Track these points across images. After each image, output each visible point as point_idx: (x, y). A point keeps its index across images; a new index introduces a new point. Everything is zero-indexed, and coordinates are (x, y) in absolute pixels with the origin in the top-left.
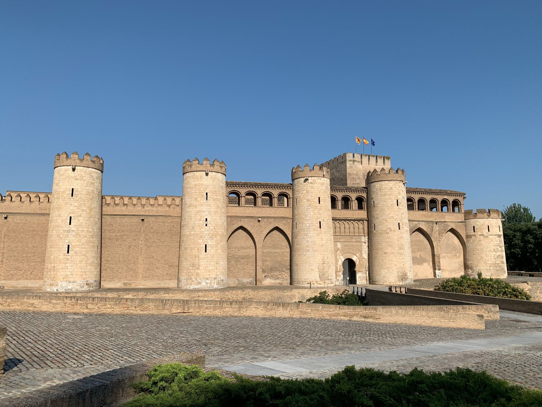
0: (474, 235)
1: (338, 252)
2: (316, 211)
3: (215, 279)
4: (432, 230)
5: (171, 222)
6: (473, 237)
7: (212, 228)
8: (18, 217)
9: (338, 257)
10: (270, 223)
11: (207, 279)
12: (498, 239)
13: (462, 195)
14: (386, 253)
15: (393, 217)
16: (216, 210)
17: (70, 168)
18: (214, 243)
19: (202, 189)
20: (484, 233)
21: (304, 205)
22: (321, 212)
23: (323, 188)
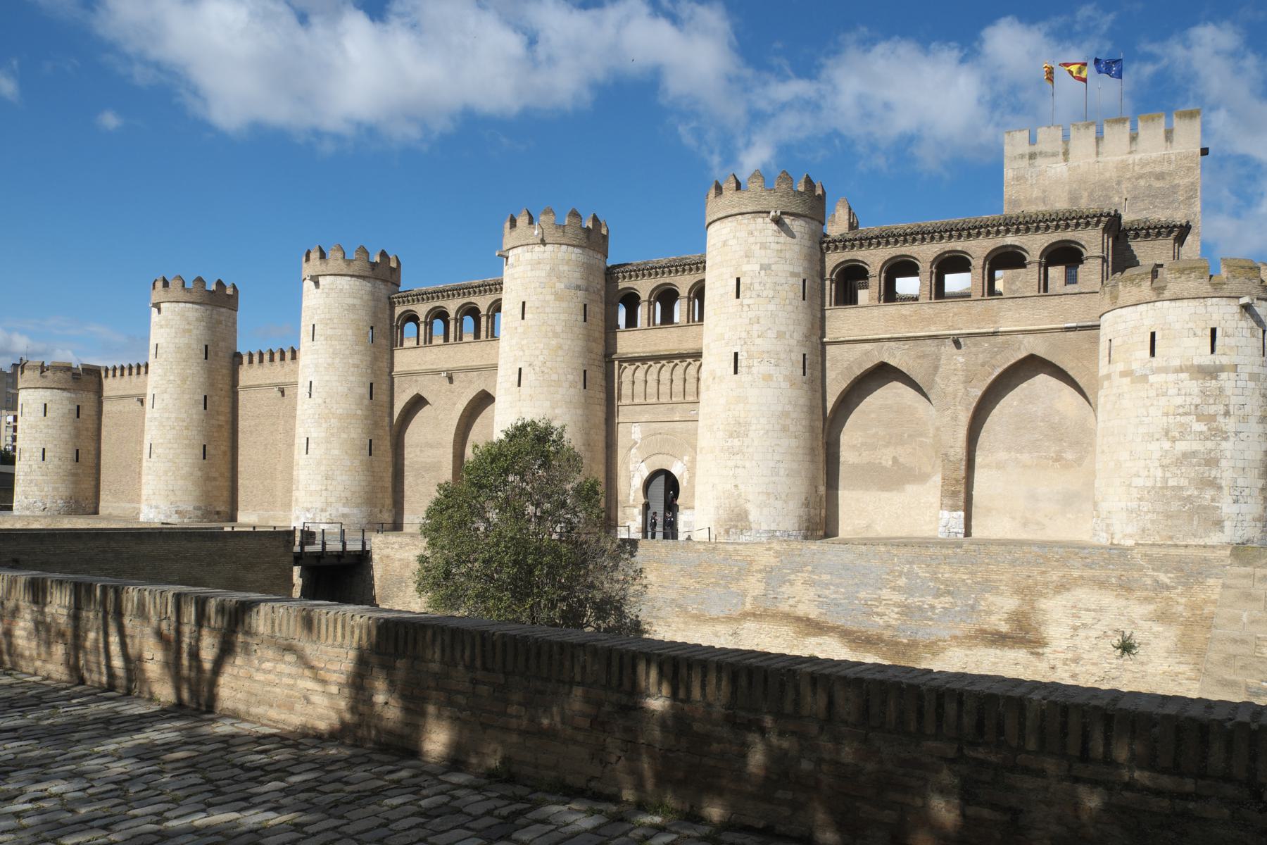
1: (634, 451)
3: (322, 510)
4: (936, 368)
7: (320, 401)
9: (631, 467)
10: (471, 382)
11: (308, 510)
12: (1193, 386)
16: (329, 361)
18: (323, 435)
20: (1135, 366)
22: (524, 342)
23: (537, 273)
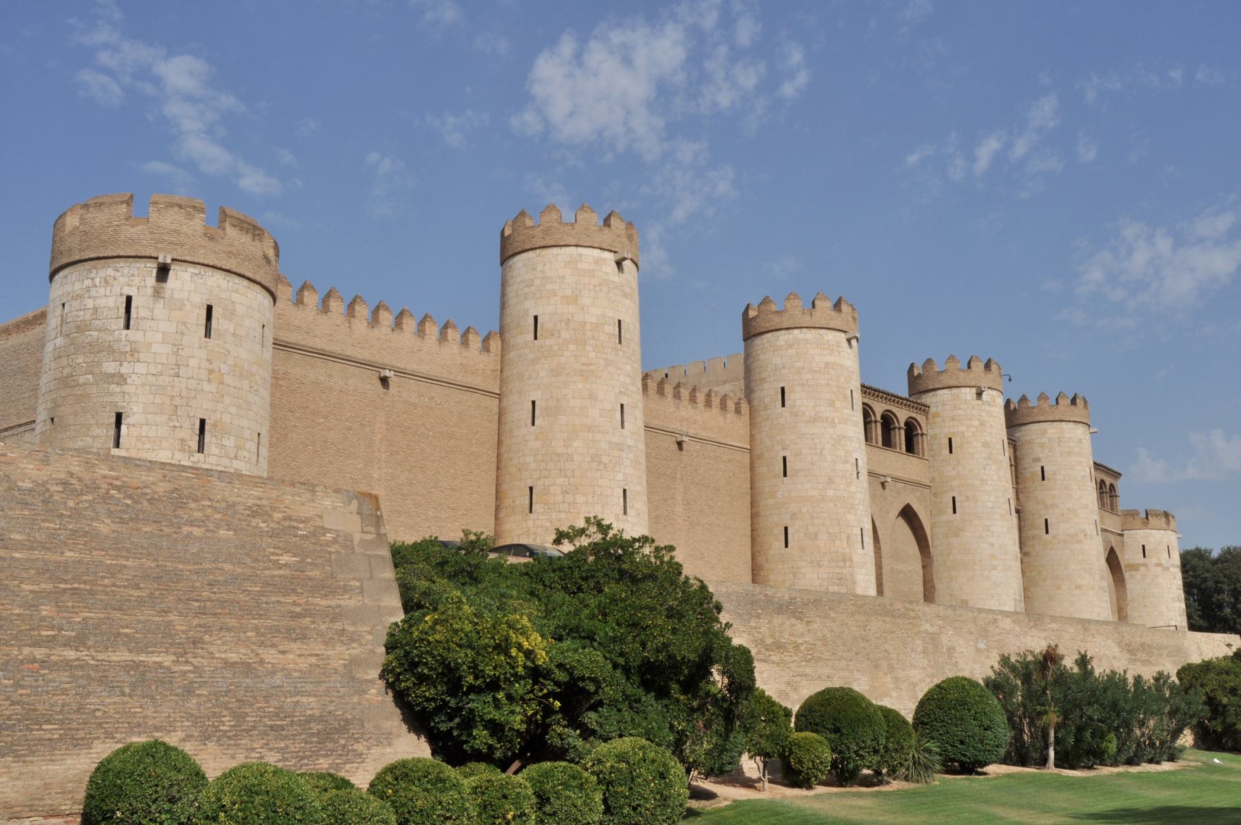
0: (1145, 565)
2: (1001, 473)
5: (729, 461)
6: (1142, 568)
8: (412, 384)
13: (1117, 475)
14: (1078, 587)
15: (1086, 507)
17: (611, 257)
19: (842, 379)
20: (1163, 561)
21: (977, 456)
